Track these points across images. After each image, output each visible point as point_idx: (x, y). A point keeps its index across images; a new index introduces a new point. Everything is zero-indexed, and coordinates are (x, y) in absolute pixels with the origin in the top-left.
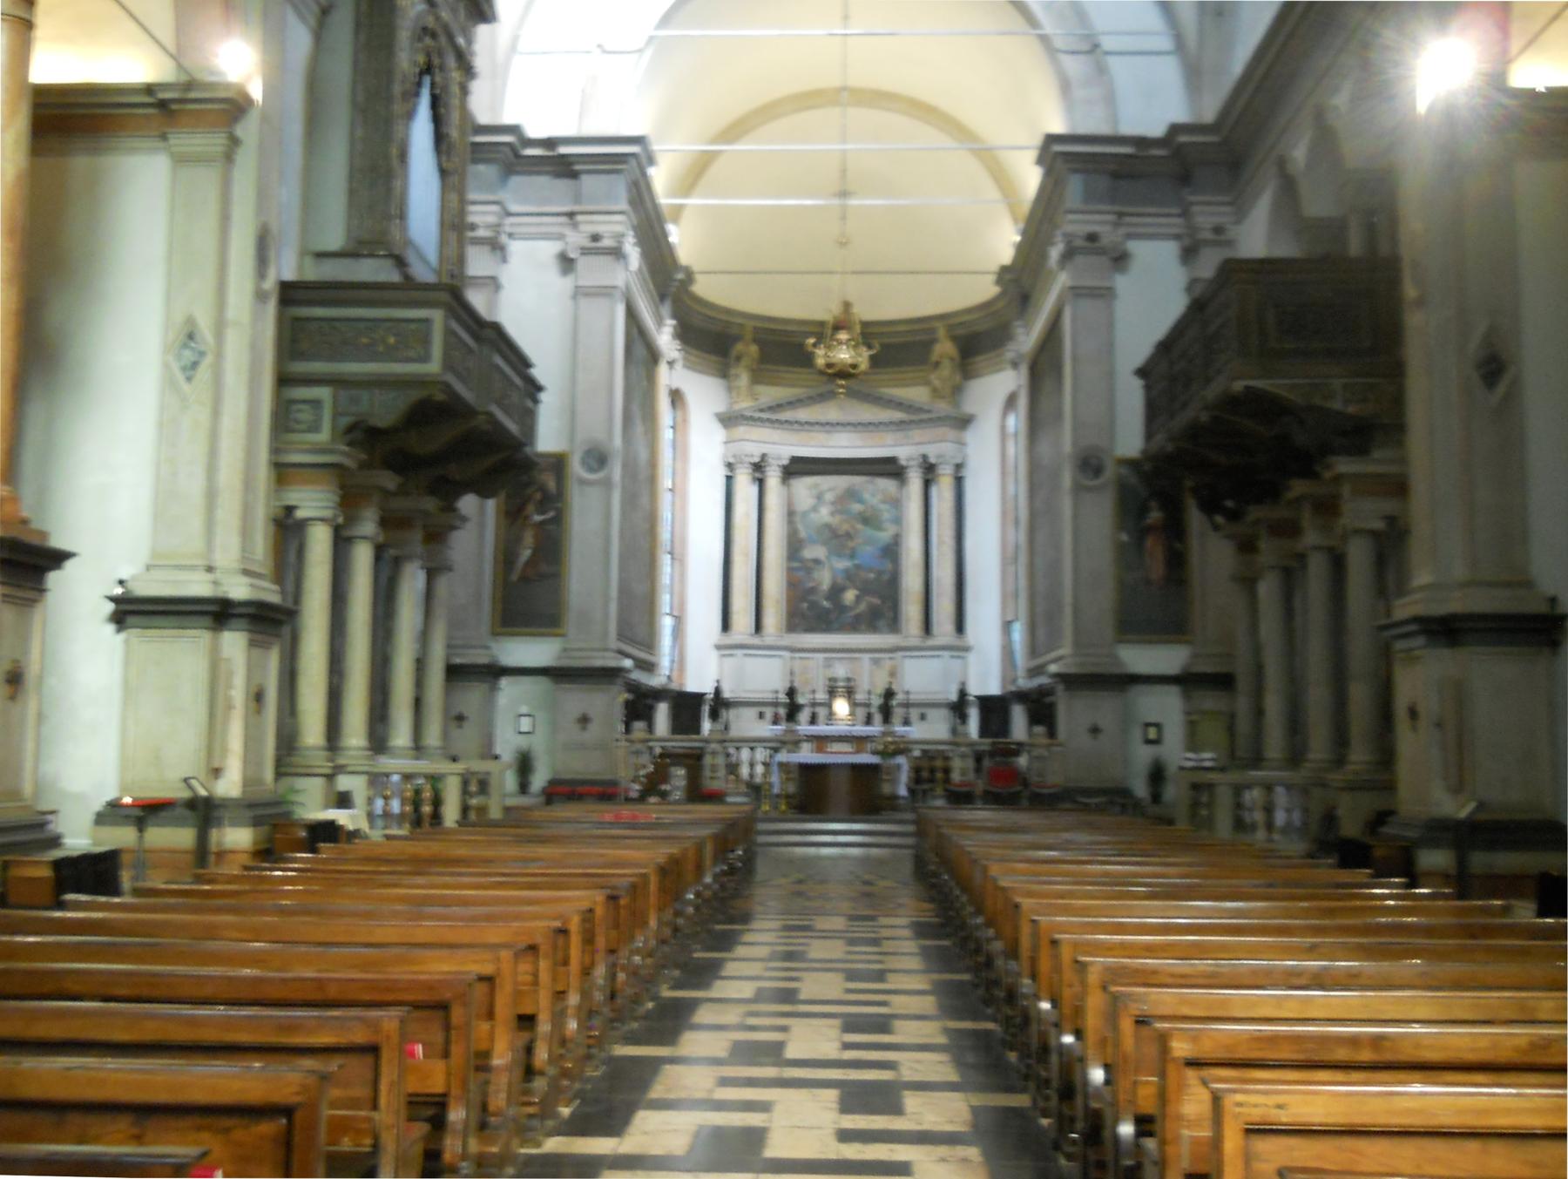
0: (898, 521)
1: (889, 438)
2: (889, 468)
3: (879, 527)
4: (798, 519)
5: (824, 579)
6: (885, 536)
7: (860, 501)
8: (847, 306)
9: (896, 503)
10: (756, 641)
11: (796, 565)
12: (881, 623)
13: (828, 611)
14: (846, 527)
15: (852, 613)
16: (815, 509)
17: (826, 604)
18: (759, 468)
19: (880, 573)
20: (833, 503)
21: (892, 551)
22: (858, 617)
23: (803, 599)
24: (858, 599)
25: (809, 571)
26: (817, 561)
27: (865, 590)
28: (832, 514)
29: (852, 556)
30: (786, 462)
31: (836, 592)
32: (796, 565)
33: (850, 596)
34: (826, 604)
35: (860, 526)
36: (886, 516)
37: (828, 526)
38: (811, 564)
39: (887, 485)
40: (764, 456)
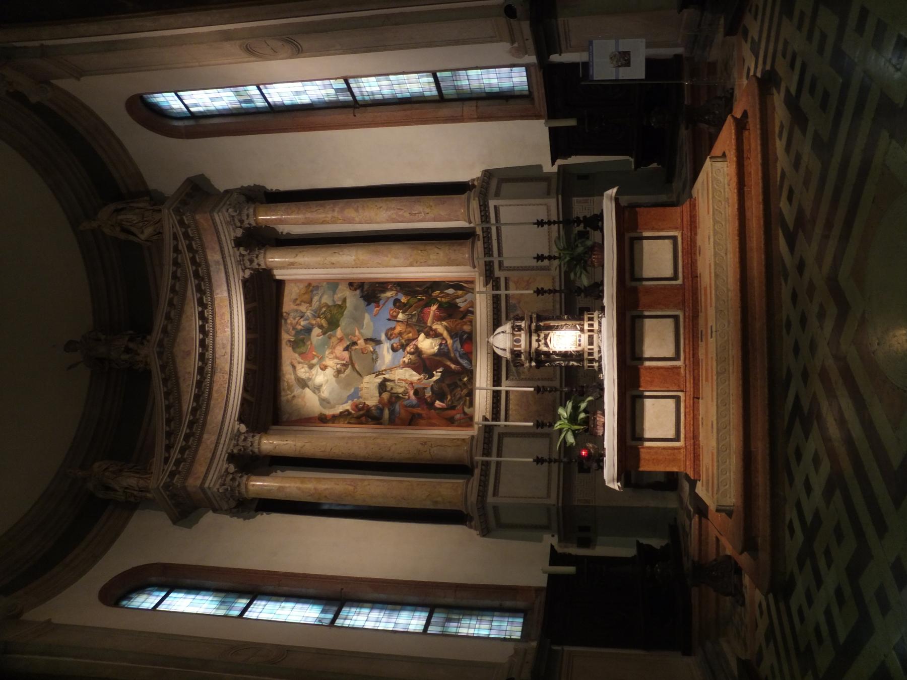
0: (333, 285)
1: (221, 294)
2: (265, 297)
3: (341, 307)
4: (329, 412)
5: (406, 377)
6: (352, 299)
7: (308, 330)
8: (70, 346)
9: (311, 287)
10: (477, 472)
11: (386, 412)
12: (462, 304)
13: (447, 372)
14: (339, 350)
15: (450, 341)
16: (317, 389)
17: (437, 375)
18: (253, 463)
19: (397, 302)
20: (311, 367)
21: (370, 292)
22: (453, 334)
23: (431, 405)
24: (432, 334)
25: (395, 398)
26: (382, 387)
27: (421, 326)
28: (324, 368)
29: (378, 342)
30: (243, 428)
31: (422, 364)
32: (386, 412)
33: (427, 345)
34: (437, 375)
35: (339, 333)
36: (326, 299)
37: (339, 372)
38: (386, 396)
39: (290, 294)
40: (232, 458)
